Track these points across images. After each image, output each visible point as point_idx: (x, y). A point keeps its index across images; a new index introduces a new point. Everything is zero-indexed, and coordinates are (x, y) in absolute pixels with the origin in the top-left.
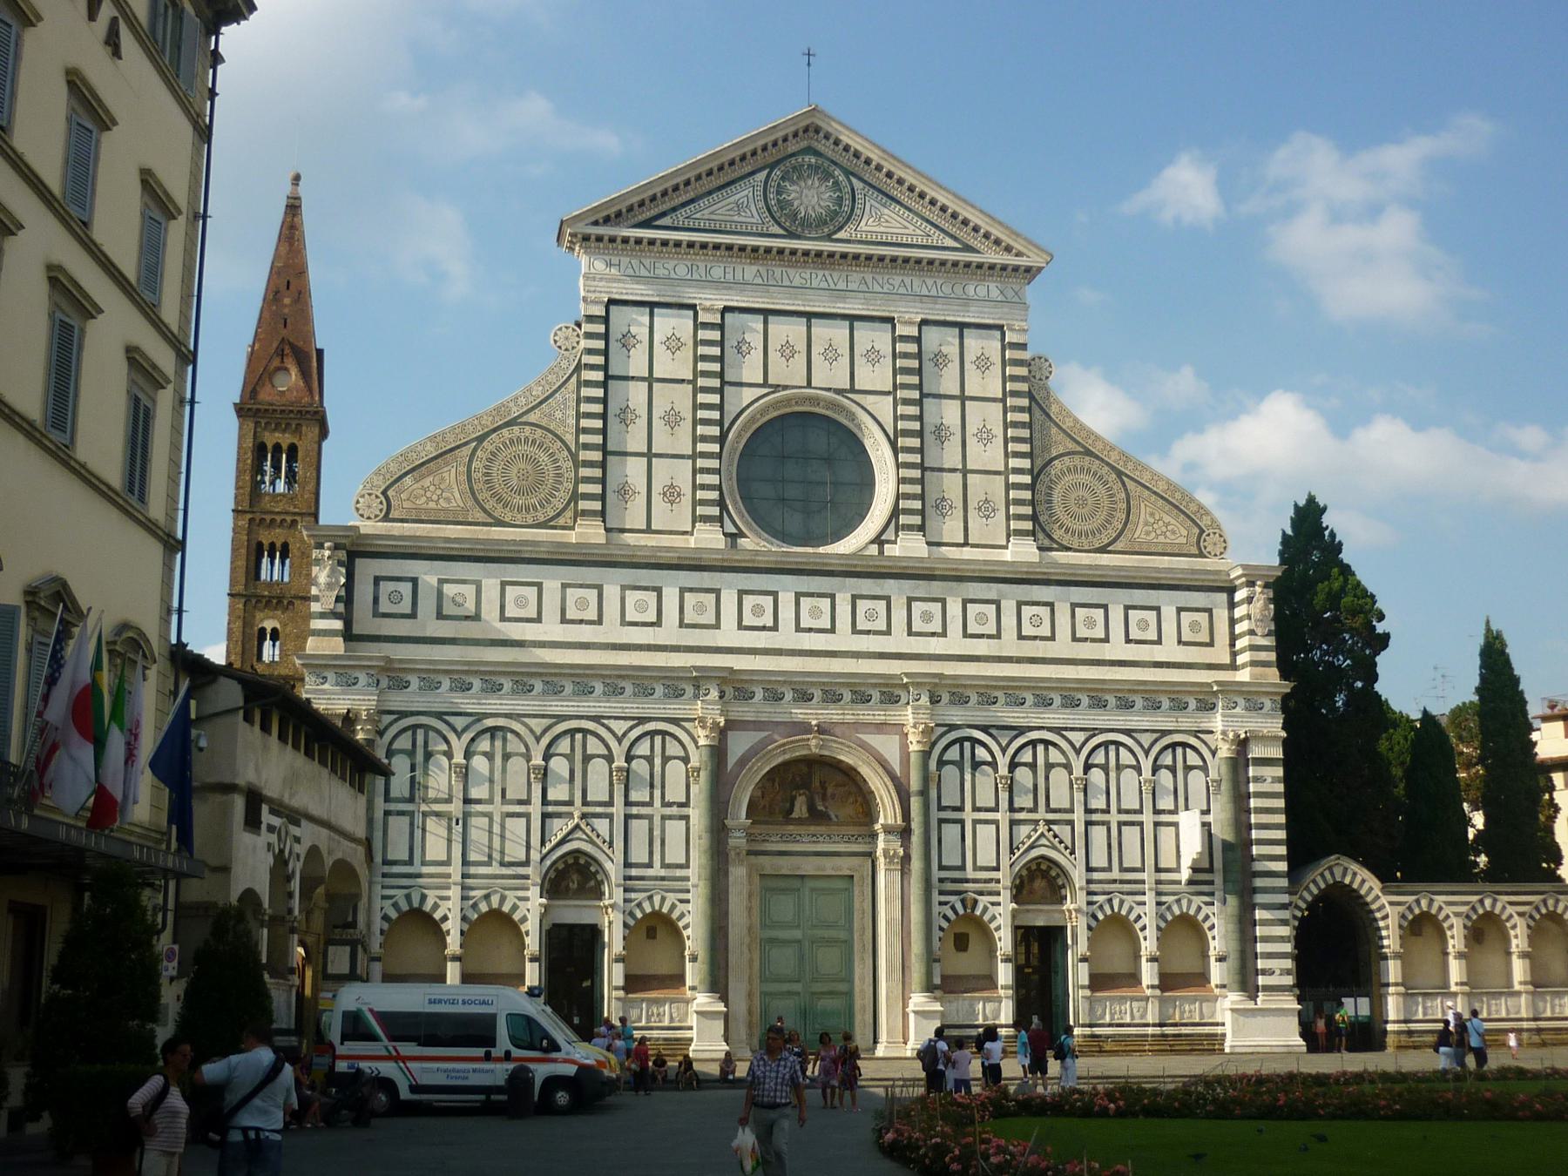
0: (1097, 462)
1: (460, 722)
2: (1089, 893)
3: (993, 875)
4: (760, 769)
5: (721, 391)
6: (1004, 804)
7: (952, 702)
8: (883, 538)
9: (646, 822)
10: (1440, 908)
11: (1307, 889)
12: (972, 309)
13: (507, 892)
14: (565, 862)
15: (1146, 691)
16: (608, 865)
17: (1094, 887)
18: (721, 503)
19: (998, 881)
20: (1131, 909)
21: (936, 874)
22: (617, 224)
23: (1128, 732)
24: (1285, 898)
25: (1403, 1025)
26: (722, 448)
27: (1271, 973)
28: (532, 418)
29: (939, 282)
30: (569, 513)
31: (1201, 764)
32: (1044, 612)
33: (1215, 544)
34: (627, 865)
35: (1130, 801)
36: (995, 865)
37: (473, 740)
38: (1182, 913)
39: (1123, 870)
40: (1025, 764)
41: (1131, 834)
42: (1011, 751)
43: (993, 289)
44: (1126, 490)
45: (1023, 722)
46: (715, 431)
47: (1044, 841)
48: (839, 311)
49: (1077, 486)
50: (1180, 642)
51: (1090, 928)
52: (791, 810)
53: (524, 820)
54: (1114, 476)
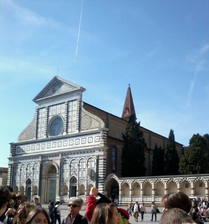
10: (128, 182)
11: (108, 179)
17: (79, 180)
23: (84, 157)
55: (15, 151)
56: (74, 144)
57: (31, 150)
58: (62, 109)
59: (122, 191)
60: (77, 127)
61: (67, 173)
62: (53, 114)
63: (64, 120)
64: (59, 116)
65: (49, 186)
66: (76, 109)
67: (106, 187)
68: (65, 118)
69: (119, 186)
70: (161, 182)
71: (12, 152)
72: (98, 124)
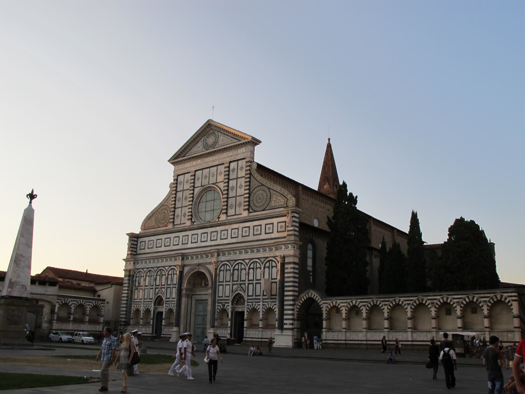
0: (264, 187)
1: (145, 270)
2: (248, 302)
3: (228, 298)
4: (188, 275)
5: (193, 190)
6: (231, 280)
7: (222, 255)
8: (220, 217)
9: (170, 289)
10: (339, 304)
11: (301, 299)
12: (239, 156)
13: (149, 305)
14: (160, 298)
15: (263, 247)
16: (164, 299)
17: (249, 301)
18: (191, 215)
19: (229, 300)
20: (257, 306)
21: (217, 298)
22: (179, 158)
24: (291, 303)
25: (345, 341)
26: (192, 203)
27: (286, 324)
28: (165, 204)
29: (233, 151)
30: (169, 223)
31: (276, 265)
32: (247, 229)
33: (291, 202)
34: (166, 298)
35: (258, 278)
36: (229, 295)
37: (147, 273)
38: (269, 307)
39: (256, 296)
40: (236, 269)
41: (258, 286)
42: (233, 266)
43: (243, 150)
44: (270, 193)
45: (236, 259)
46: (191, 199)
47: (239, 289)
48: (214, 165)
49: (259, 194)
50: (278, 232)
51: (247, 311)
52: (201, 285)
53: (152, 289)
54: (268, 190)
55: (136, 248)
56: (240, 236)
57: (163, 245)
58: (218, 175)
59: (327, 320)
60: (245, 206)
61: (228, 287)
62: (202, 185)
63: (223, 195)
64: (214, 187)
65: (193, 310)
66: (244, 175)
67: (297, 314)
68: (224, 190)
69: (322, 311)
70: (401, 305)
71: (131, 249)
72: (283, 201)
